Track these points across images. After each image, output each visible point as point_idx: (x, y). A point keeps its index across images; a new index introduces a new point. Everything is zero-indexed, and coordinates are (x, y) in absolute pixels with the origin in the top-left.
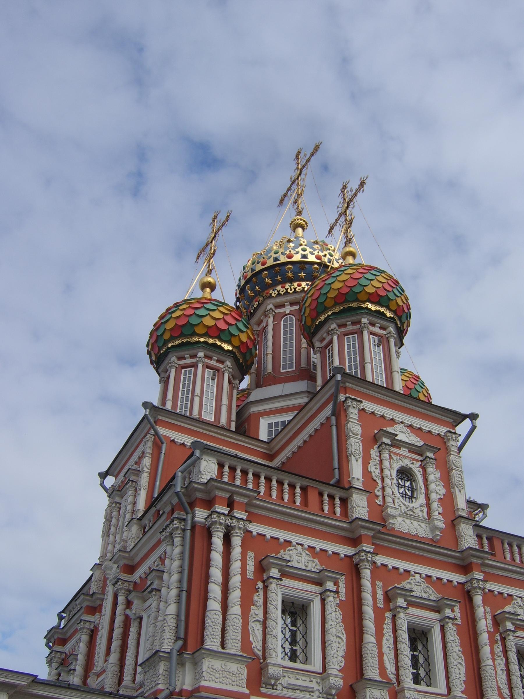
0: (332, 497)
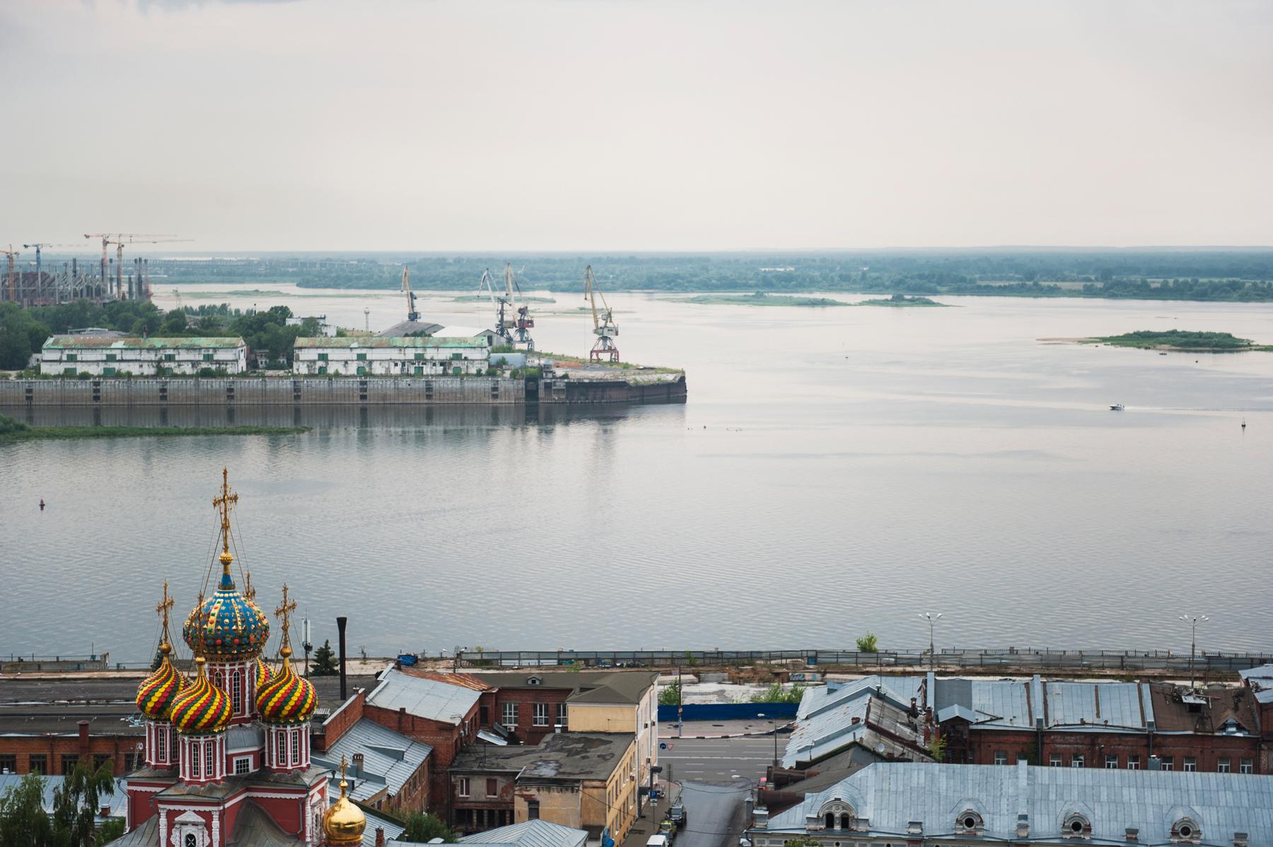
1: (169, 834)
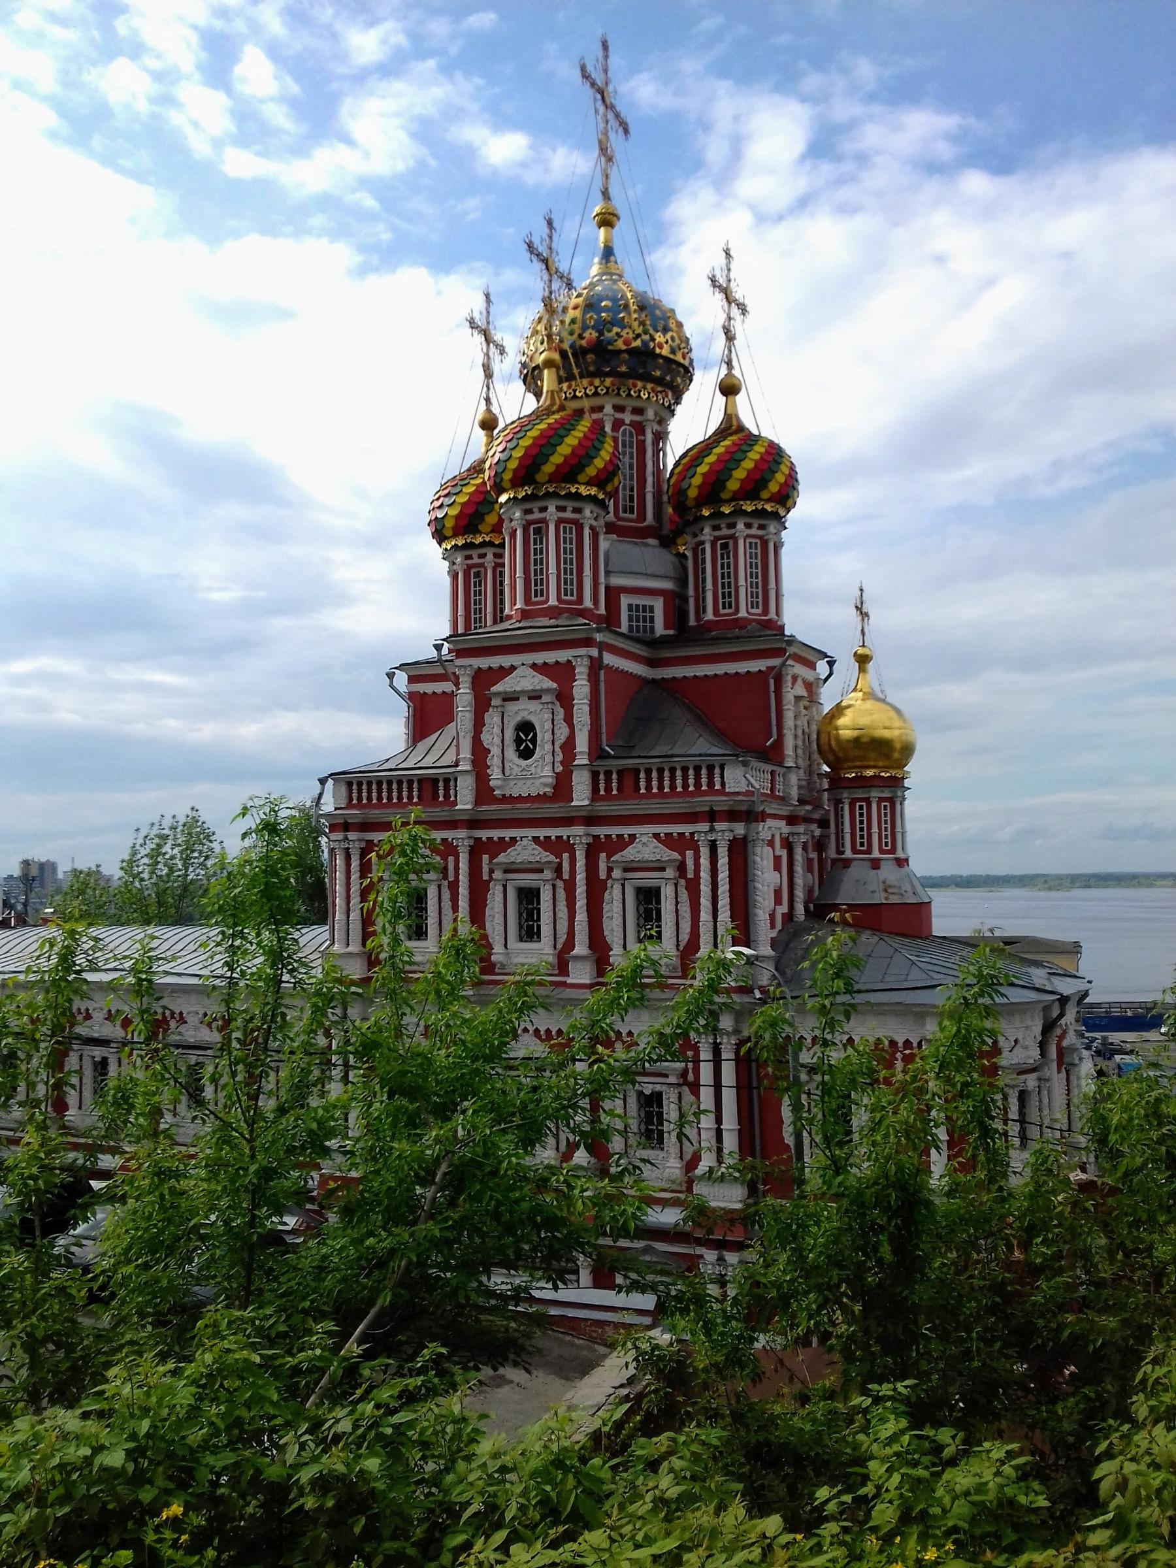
0: (447, 781)
1: (479, 724)
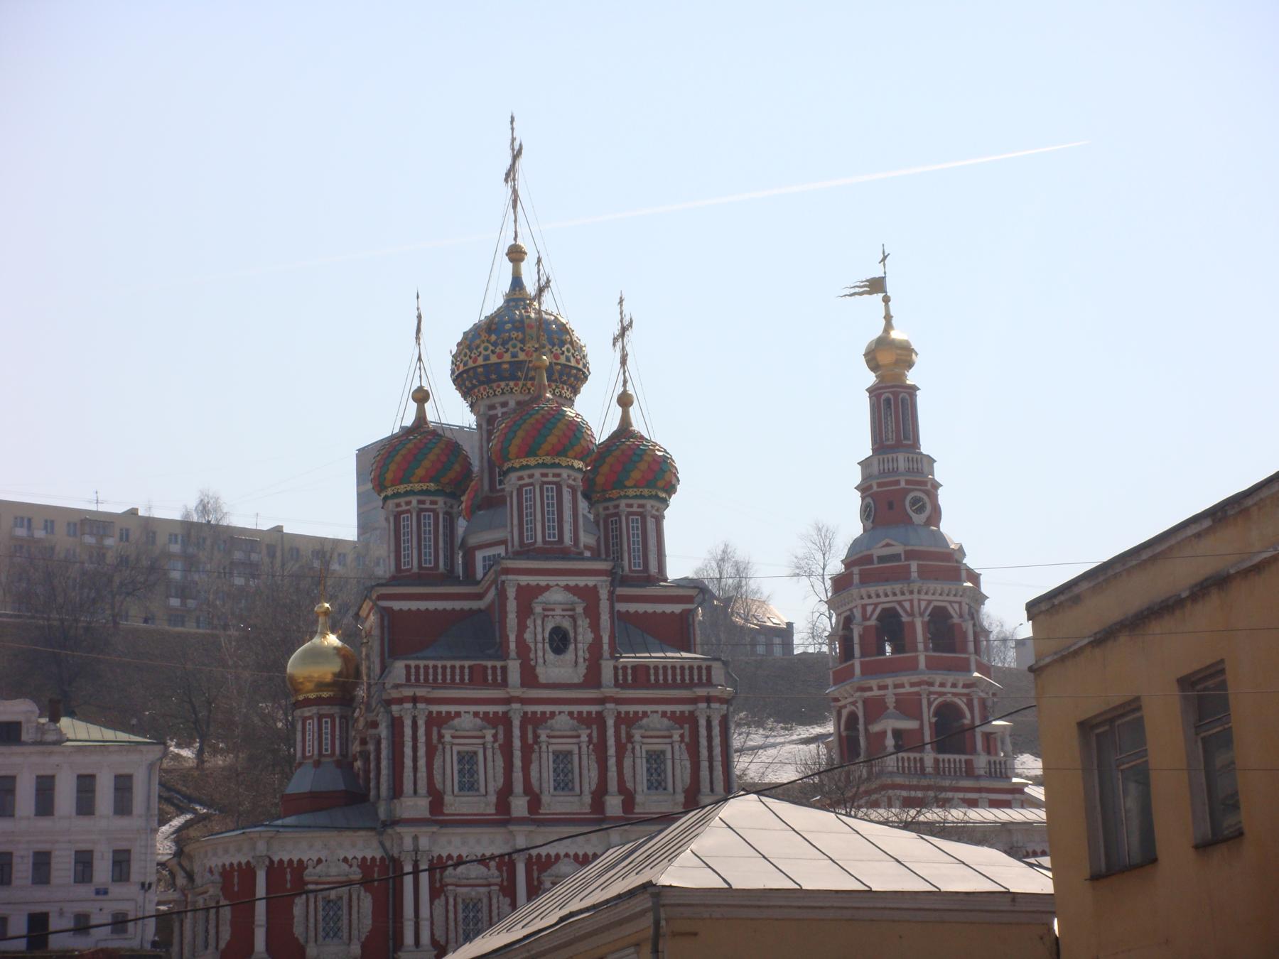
1: (522, 627)
